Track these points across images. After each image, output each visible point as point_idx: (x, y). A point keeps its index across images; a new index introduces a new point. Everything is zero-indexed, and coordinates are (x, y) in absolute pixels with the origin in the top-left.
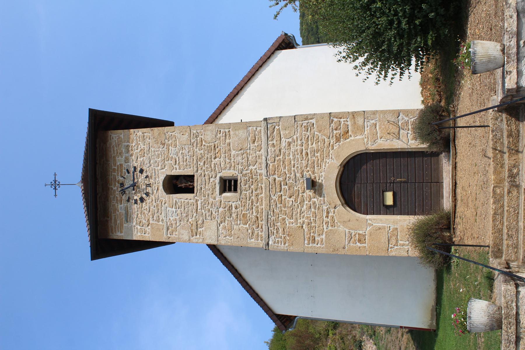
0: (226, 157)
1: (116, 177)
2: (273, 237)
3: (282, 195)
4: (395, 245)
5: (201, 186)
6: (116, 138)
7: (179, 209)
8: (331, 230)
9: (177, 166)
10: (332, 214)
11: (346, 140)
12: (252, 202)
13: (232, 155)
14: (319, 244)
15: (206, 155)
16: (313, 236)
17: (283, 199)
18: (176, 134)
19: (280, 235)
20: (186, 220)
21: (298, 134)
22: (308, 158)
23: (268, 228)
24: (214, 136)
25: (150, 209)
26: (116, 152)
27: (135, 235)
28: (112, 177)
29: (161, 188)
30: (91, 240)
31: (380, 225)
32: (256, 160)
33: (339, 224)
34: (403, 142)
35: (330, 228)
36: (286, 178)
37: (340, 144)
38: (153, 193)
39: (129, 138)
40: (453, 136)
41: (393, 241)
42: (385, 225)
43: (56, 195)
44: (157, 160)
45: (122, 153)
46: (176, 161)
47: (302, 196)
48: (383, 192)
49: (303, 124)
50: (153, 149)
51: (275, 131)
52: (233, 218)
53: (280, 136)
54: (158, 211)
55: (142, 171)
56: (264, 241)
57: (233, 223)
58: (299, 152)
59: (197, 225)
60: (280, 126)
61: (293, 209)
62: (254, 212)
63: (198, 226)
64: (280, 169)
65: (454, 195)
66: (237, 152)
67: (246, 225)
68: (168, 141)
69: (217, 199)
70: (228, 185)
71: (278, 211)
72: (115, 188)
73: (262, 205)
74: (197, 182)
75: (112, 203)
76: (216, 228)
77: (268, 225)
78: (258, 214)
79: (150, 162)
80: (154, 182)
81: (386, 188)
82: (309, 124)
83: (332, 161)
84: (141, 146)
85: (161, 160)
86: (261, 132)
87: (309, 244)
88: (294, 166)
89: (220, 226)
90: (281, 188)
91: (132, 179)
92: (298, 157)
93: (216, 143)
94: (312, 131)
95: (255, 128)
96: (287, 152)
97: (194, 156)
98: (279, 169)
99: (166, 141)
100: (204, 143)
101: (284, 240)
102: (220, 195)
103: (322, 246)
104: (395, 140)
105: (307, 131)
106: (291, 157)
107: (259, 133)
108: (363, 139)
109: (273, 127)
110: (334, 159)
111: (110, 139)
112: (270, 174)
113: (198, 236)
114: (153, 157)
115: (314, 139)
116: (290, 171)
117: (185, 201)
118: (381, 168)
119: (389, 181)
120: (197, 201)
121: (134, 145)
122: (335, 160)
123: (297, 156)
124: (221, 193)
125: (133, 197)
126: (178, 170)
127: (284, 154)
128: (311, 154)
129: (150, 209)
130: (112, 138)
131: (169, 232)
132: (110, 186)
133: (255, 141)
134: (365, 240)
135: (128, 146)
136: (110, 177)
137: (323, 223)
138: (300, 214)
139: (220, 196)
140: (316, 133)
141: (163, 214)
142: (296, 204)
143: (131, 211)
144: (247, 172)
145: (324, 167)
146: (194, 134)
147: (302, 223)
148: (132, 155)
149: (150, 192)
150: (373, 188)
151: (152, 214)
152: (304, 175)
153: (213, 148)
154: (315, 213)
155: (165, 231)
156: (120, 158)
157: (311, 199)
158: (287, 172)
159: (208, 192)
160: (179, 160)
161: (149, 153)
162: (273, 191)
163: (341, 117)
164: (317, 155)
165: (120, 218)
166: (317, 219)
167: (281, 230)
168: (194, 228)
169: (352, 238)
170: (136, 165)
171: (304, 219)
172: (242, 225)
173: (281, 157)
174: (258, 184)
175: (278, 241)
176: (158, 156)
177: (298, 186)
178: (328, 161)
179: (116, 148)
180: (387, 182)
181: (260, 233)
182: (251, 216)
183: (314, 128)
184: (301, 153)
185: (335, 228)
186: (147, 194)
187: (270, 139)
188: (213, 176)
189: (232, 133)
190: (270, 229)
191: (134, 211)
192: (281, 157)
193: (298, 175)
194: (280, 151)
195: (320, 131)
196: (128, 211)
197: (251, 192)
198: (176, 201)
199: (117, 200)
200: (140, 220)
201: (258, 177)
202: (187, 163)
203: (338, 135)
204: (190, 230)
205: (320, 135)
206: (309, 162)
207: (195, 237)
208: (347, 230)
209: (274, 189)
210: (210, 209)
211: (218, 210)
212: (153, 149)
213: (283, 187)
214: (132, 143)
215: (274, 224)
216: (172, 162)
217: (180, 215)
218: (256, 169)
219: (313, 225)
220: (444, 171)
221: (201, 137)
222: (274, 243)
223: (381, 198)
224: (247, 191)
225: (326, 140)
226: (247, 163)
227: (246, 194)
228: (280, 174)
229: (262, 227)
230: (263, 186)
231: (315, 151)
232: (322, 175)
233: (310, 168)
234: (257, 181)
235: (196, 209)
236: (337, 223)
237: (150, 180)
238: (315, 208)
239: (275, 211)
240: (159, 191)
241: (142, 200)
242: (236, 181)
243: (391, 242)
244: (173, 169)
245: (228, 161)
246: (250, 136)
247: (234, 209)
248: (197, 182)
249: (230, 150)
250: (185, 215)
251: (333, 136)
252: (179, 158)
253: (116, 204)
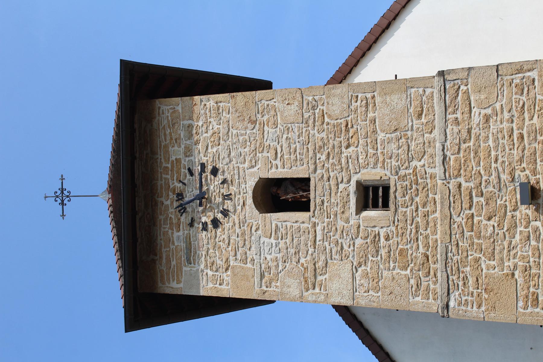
0: (367, 145)
1: (169, 182)
2: (457, 294)
3: (473, 214)
5: (322, 198)
6: (168, 111)
7: (282, 239)
9: (278, 162)
12: (417, 227)
13: (379, 141)
15: (331, 141)
16: (534, 293)
18: (276, 104)
19: (471, 289)
21: (505, 100)
22: (522, 145)
24: (345, 106)
25: (229, 241)
26: (168, 138)
27: (204, 286)
29: (250, 201)
30: (126, 296)
32: (424, 149)
36: (481, 184)
38: (235, 211)
39: (192, 112)
43: (63, 215)
45: (179, 138)
47: (513, 217)
49: (514, 81)
50: (235, 132)
51: (460, 94)
52: (381, 258)
53: (470, 104)
54: (244, 244)
55: (215, 171)
56: (439, 301)
57: (381, 266)
58: (506, 134)
59: (315, 270)
60: (469, 86)
61: (494, 242)
63: (318, 271)
64: (470, 167)
66: (388, 135)
67: (406, 269)
68: (262, 117)
69: (352, 222)
71: (465, 244)
73: (435, 232)
75: (162, 230)
76: (350, 275)
78: (428, 250)
80: (237, 191)
82: (524, 80)
84: (213, 126)
85: (250, 151)
86: (432, 96)
87: (526, 307)
88: (496, 161)
89: (357, 271)
90: (472, 201)
91: (198, 185)
92: (503, 144)
93: (349, 119)
94: (532, 94)
95: (421, 90)
97: (310, 144)
98: (468, 166)
99: (259, 116)
100: (327, 119)
101: (478, 299)
102: (356, 214)
105: (522, 93)
106: (491, 143)
107: (428, 99)
109: (456, 87)
111: (159, 114)
113: (317, 290)
115: (534, 109)
116: (488, 169)
117: (294, 225)
121: (200, 124)
123: (501, 141)
124: (359, 211)
125: (200, 218)
126: (280, 170)
127: (478, 138)
128: (529, 137)
129: (229, 241)
131: (264, 281)
132: (160, 199)
133: (421, 114)
135: (190, 126)
136: (159, 183)
138: (509, 251)
139: (358, 216)
141: (253, 249)
143: (196, 243)
144: (407, 172)
146: (308, 104)
147: (512, 268)
148: (197, 143)
149: (231, 208)
151: (234, 248)
153: (343, 129)
154: (539, 250)
155: (257, 280)
156: (176, 148)
157: (530, 222)
158: (482, 172)
159: (335, 209)
160: (282, 150)
161: (228, 139)
162: (456, 207)
165: (176, 256)
167: (471, 281)
170: (204, 160)
171: (516, 260)
172: (399, 271)
173: (471, 144)
174: (428, 195)
175: (466, 300)
177: (504, 199)
179: (169, 131)
181: (432, 286)
182: (414, 254)
183: (535, 88)
186: (225, 213)
187: (450, 110)
188: (345, 180)
189: (378, 99)
190: (450, 277)
191: (201, 244)
192: (471, 144)
193: (504, 177)
194: (469, 131)
196: (190, 243)
197: (414, 210)
198: (277, 226)
199: (171, 224)
201: (429, 181)
202: (296, 157)
204: (302, 279)
206: (526, 152)
207: (311, 291)
209: (458, 203)
210: (340, 241)
211: (354, 243)
212: (235, 132)
213: (475, 200)
214: (198, 121)
215: (459, 270)
216: (269, 155)
217: (285, 251)
218: (424, 165)
219: (533, 271)
221: (322, 108)
222: (460, 304)
224: (407, 207)
226: (408, 154)
227: (405, 212)
228: (470, 175)
229: (435, 275)
230: (438, 197)
231: (536, 131)
234: (426, 189)
235: (313, 240)
237: (231, 187)
239: (460, 244)
240: (247, 207)
241: (216, 223)
242: (386, 189)
244: (272, 167)
245: (371, 151)
247: (382, 239)
249: (375, 132)
250: (292, 251)
252: (282, 147)
253: (170, 231)
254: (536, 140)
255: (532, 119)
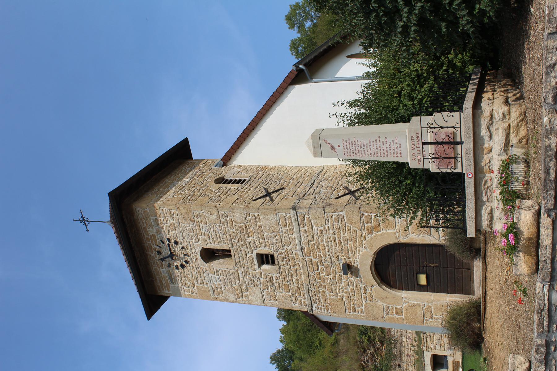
0: (259, 237)
1: (151, 245)
2: (316, 305)
3: (319, 273)
4: (430, 318)
5: (239, 259)
6: (142, 211)
7: (221, 276)
8: (369, 303)
9: (211, 241)
10: (370, 291)
11: (377, 232)
12: (292, 275)
13: (265, 236)
14: (360, 313)
15: (238, 234)
16: (353, 307)
17: (321, 276)
18: (204, 213)
19: (323, 304)
20: (230, 286)
21: (329, 224)
22: (341, 245)
23: (310, 298)
24: (243, 218)
25: (192, 275)
26: (145, 224)
27: (183, 294)
28: (148, 245)
29: (199, 258)
30: (141, 297)
31: (415, 302)
32: (290, 241)
33: (377, 299)
34: (435, 238)
35: (369, 302)
36: (322, 261)
37: (373, 235)
38: (192, 261)
39: (156, 213)
40: (484, 254)
41: (428, 315)
42: (420, 303)
43: (87, 230)
44: (190, 234)
45: (152, 225)
46: (209, 237)
47: (340, 276)
48: (417, 274)
49: (334, 216)
50: (183, 225)
51: (306, 219)
52: (275, 287)
53: (312, 224)
54: (201, 277)
55: (176, 243)
56: (307, 307)
57: (276, 290)
58: (332, 240)
59: (241, 290)
60: (310, 216)
61: (332, 285)
62: (295, 284)
63: (243, 291)
64: (315, 252)
65: (484, 301)
66: (269, 234)
67: (289, 292)
68: (197, 219)
69: (257, 271)
70: (265, 259)
71: (317, 285)
72: (153, 255)
73: (301, 278)
74: (234, 256)
75: (153, 268)
76: (260, 293)
77: (309, 295)
78: (299, 285)
79: (183, 236)
80: (191, 252)
81: (420, 271)
82: (339, 216)
83: (366, 250)
84: (170, 221)
85: (194, 235)
86: (291, 218)
87: (350, 312)
88: (329, 251)
89: (263, 292)
90: (318, 267)
91: (168, 248)
92: (331, 244)
93: (247, 224)
94: (343, 222)
95: (284, 214)
96: (320, 239)
97: (227, 234)
98: (314, 252)
99: (195, 218)
100: (234, 224)
101: (327, 308)
102: (259, 268)
103: (362, 315)
104: (426, 236)
105: (338, 222)
106: (325, 242)
107: (289, 219)
108: (395, 233)
109: (303, 216)
110: (367, 248)
111: (136, 212)
112: (305, 256)
113: (244, 299)
114: (185, 232)
115: (345, 229)
116: (325, 255)
117: (226, 270)
118: (414, 255)
119: (421, 265)
120: (237, 271)
121: (162, 219)
122: (368, 249)
123: (330, 243)
124: (259, 266)
125: (173, 263)
126: (213, 245)
127: (318, 240)
128: (344, 242)
129: (192, 275)
130: (137, 211)
131: (215, 293)
132: (148, 253)
133: (286, 225)
134: (402, 313)
135: (156, 220)
136: (146, 245)
137: (361, 297)
138: (339, 289)
139: (260, 269)
140: (347, 224)
141: (206, 278)
142: (335, 282)
143: (174, 274)
144: (283, 251)
145: (358, 254)
146: (222, 215)
147: (342, 296)
148: (163, 228)
149: (189, 260)
150: (407, 269)
151: (195, 278)
152: (340, 259)
153: (244, 229)
154: (354, 290)
155: (211, 293)
156: (151, 229)
157: (348, 278)
158: (322, 256)
159: (247, 265)
160: (212, 236)
161: (180, 228)
162: (311, 269)
163: (371, 212)
164: (350, 243)
165: (165, 279)
166: (355, 294)
167: (322, 300)
168: (239, 291)
169: (389, 310)
170: (169, 236)
171: (343, 293)
172: (285, 293)
173: (315, 242)
174: (295, 262)
175: (321, 308)
176: (190, 231)
177: (334, 267)
178: (361, 249)
179: (145, 221)
180: (420, 266)
181: (303, 300)
182: (292, 286)
183: (345, 220)
184: (334, 241)
185: (374, 302)
186: (187, 262)
187: (301, 226)
188: (250, 252)
189: (261, 217)
190: (312, 298)
191: (177, 275)
192: (315, 242)
193: (333, 258)
194: (313, 237)
195: (351, 224)
196: (171, 274)
197: (289, 268)
198: (217, 270)
199: (158, 265)
200: (185, 282)
201: (294, 256)
202: (221, 239)
203: (369, 228)
204: (235, 294)
205: (351, 227)
206: (343, 248)
207: (241, 299)
208: (385, 305)
209: (311, 268)
210: (252, 279)
211: (260, 280)
212: (183, 225)
213: (320, 267)
214: (160, 217)
215: (315, 295)
216: (205, 237)
217: (224, 281)
218: (291, 249)
219: (352, 298)
220: (474, 265)
221: (230, 217)
222: (318, 309)
223: (415, 280)
224: (285, 266)
225: (358, 231)
226: (282, 243)
227: (284, 268)
228: (316, 256)
229: (304, 296)
230: (300, 264)
231: (347, 240)
232: (357, 261)
233: (345, 254)
234: (294, 259)
235: (238, 277)
236: (374, 298)
237: (187, 250)
238: (353, 286)
239: (315, 285)
240: (198, 260)
241: (183, 266)
242: (272, 256)
243: (426, 316)
244: (208, 243)
245: (261, 240)
246: (281, 221)
247: (274, 279)
248: (234, 256)
249: (262, 232)
250: (228, 281)
251: (364, 229)
252: (212, 234)
253: (158, 268)
254: (348, 244)
255: (345, 234)
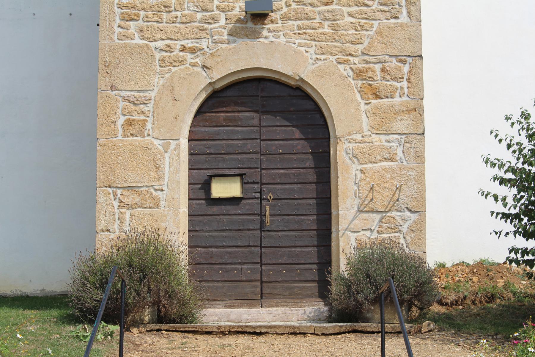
4: (121, 202)
8: (153, 56)
10: (189, 61)
11: (359, 92)
14: (121, 30)
16: (138, 16)
31: (167, 169)
33: (167, 76)
34: (352, 221)
37: (350, 79)
40: (365, 329)
41: (130, 198)
42: (166, 180)
48: (241, 175)
65: (233, 330)
81: (248, 183)
82: (397, 7)
83: (311, 61)
94: (380, 15)
104: (357, 202)
105: (381, 4)
108: (360, 131)
110: (316, 65)
115: (362, 18)
118: (293, 171)
119: (264, 188)
122: (313, 67)
128: (328, 12)
134: (132, 135)
137: (169, 39)
140: (376, 24)
150: (250, 153)
154: (191, 22)
157: (224, 12)
163: (413, 81)
164: (326, 27)
166: (177, 25)
178: (312, 50)
180: (262, 184)
183: (387, 19)
195: (379, 33)
203: (370, 74)
206: (310, 8)
208: (152, 95)
219: (165, 16)
220: (288, 308)
225: (360, 47)
231: (335, 20)
232: (279, 37)
233: (295, 10)
236: (170, 70)
238: (203, 21)
243: (127, 193)
251: (367, 63)
254: (324, 20)
255: (349, 15)
